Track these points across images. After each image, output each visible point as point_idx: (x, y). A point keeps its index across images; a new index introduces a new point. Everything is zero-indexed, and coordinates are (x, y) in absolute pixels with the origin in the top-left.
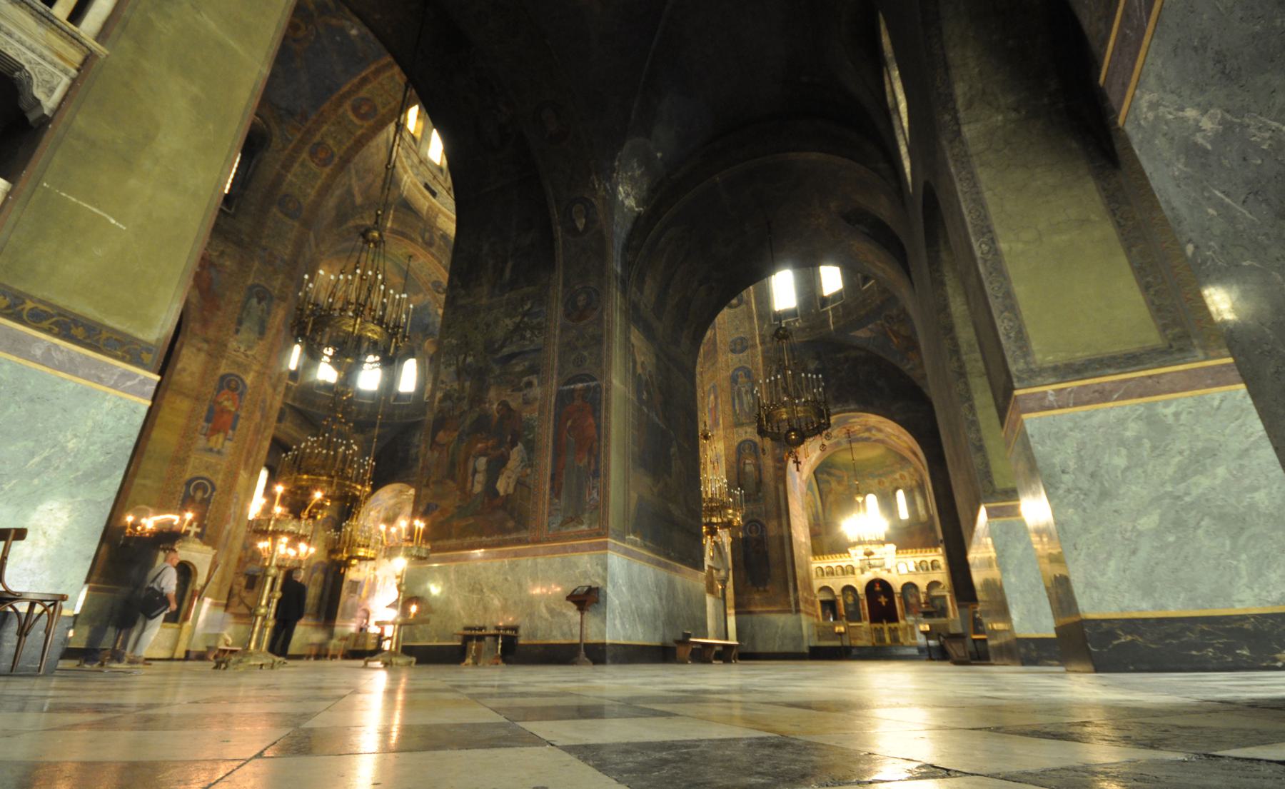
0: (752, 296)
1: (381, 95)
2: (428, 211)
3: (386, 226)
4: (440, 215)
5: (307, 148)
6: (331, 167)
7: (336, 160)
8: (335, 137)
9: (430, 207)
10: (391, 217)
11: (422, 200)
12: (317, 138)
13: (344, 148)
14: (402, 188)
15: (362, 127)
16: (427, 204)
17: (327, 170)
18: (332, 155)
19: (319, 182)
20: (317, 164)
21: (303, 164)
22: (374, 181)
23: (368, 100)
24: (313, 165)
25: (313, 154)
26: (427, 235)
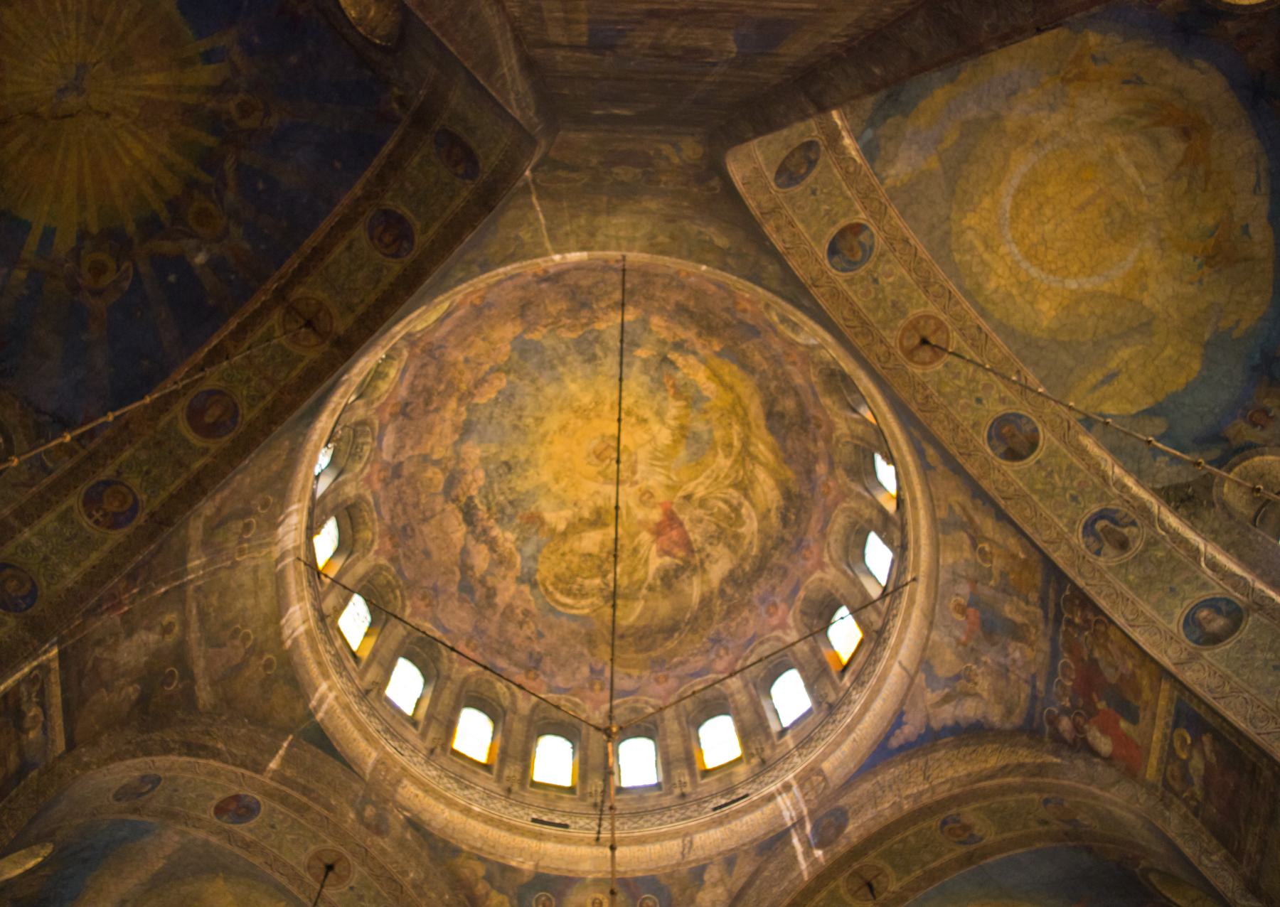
0: (1259, 585)
1: (249, 380)
2: (375, 768)
3: (266, 766)
4: (405, 782)
5: (83, 488)
6: (126, 530)
7: (141, 519)
8: (147, 473)
9: (380, 762)
10: (281, 752)
11: (363, 745)
12: (108, 472)
13: (164, 495)
14: (313, 703)
15: (205, 451)
16: (374, 755)
17: (118, 536)
18: (134, 509)
19: (94, 558)
20: (97, 522)
21: (64, 518)
22: (244, 663)
23: (220, 393)
24: (86, 522)
25: (91, 501)
26: (369, 811)
